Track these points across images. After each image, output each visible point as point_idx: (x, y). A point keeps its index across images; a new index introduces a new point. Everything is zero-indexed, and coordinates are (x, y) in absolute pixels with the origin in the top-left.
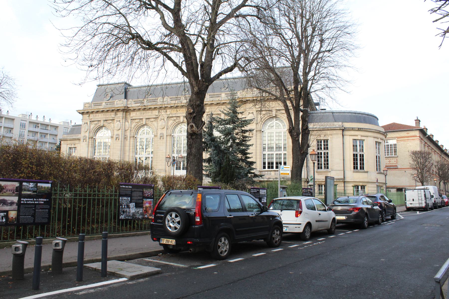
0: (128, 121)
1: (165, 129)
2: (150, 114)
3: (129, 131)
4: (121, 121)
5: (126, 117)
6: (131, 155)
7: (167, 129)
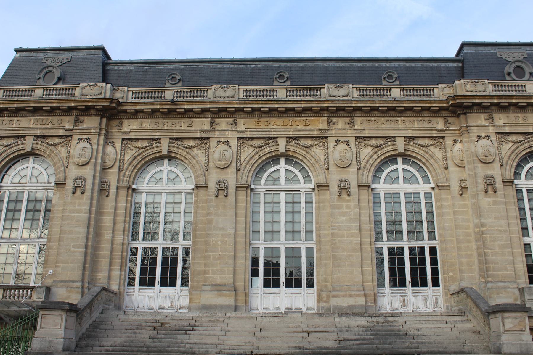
0: (113, 144)
1: (232, 170)
2: (184, 126)
3: (115, 170)
4: (94, 141)
5: (107, 132)
6: (119, 239)
7: (238, 170)
